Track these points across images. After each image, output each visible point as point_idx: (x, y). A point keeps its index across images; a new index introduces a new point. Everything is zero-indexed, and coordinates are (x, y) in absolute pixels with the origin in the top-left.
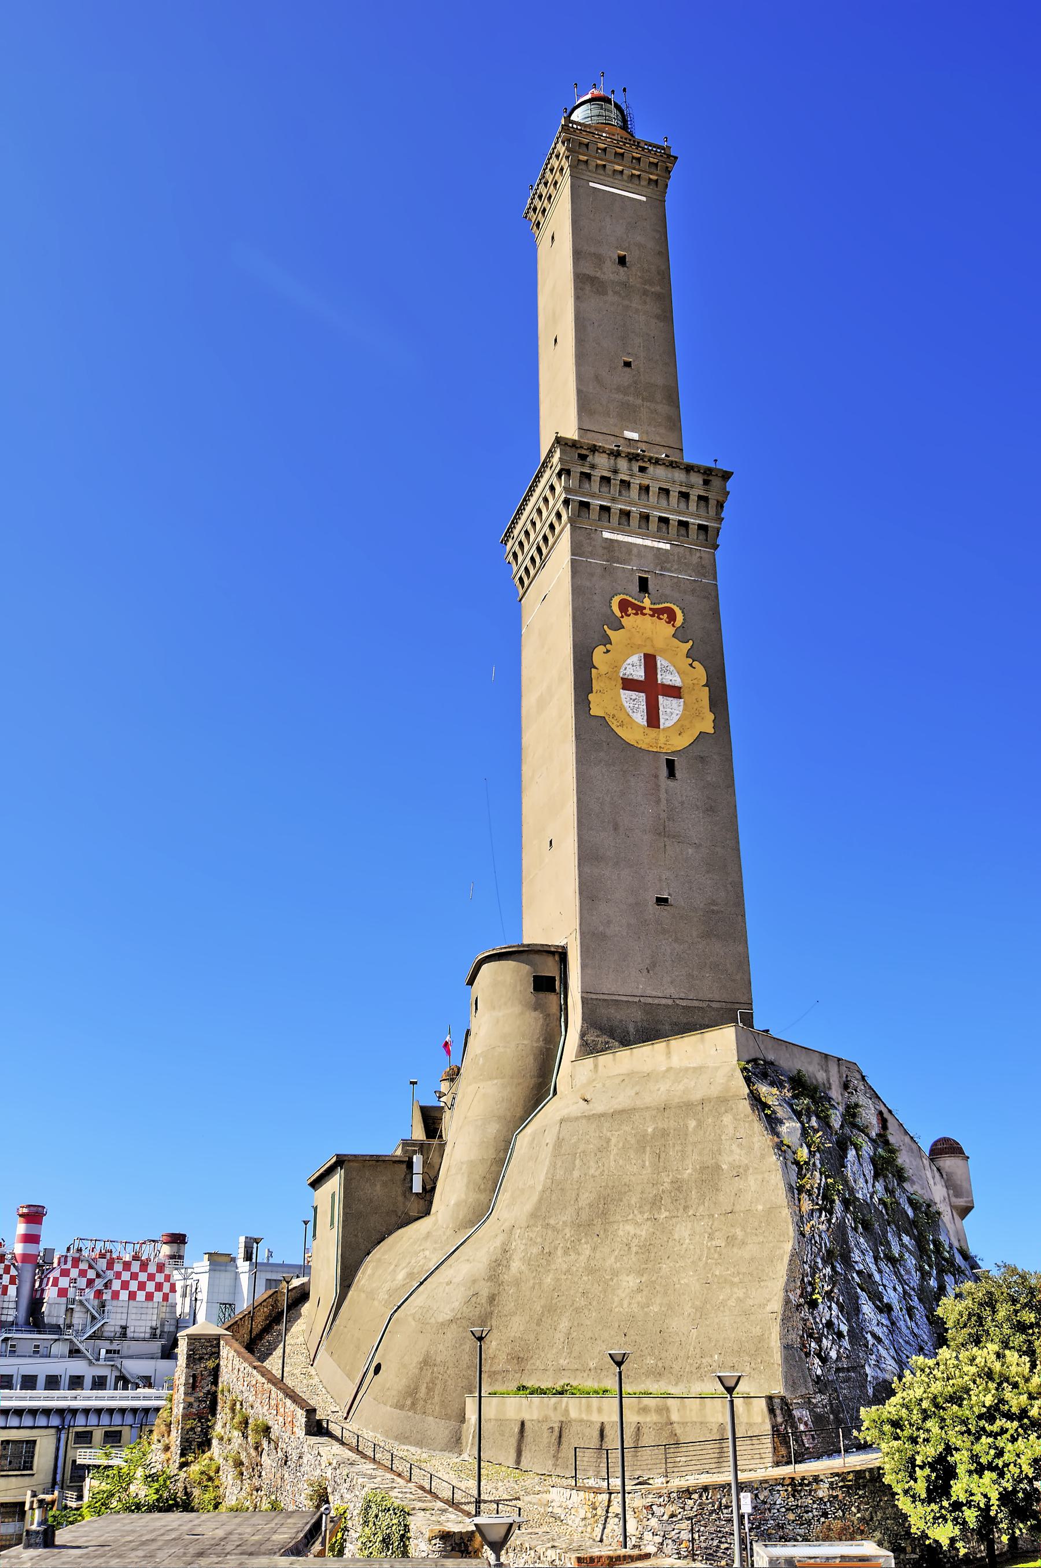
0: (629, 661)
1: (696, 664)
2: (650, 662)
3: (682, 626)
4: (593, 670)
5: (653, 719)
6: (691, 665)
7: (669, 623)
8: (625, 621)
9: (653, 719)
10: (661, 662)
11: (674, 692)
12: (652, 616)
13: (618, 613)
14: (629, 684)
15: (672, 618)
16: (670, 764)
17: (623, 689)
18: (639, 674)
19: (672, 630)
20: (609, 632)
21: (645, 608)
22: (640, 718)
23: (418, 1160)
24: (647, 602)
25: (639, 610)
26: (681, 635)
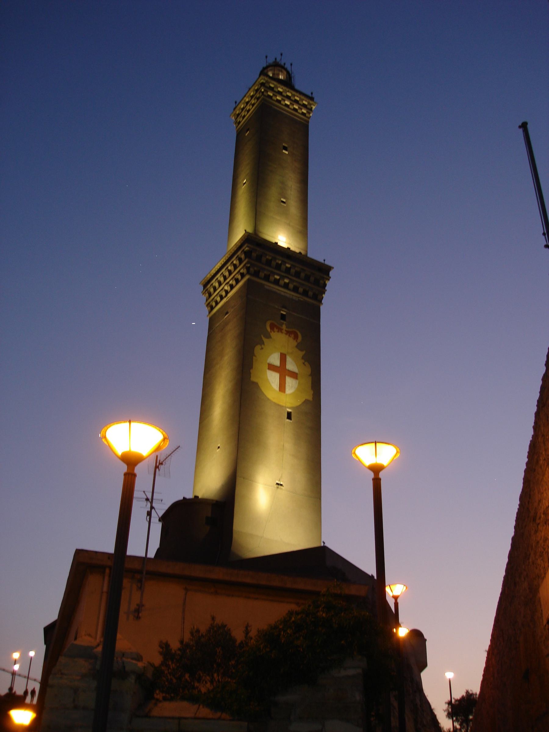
1: (306, 363)
2: (283, 358)
4: (254, 357)
5: (282, 388)
6: (304, 363)
8: (273, 334)
9: (282, 388)
10: (289, 359)
11: (294, 375)
12: (286, 334)
14: (272, 367)
17: (269, 369)
18: (277, 363)
19: (295, 344)
25: (280, 330)
26: (299, 347)
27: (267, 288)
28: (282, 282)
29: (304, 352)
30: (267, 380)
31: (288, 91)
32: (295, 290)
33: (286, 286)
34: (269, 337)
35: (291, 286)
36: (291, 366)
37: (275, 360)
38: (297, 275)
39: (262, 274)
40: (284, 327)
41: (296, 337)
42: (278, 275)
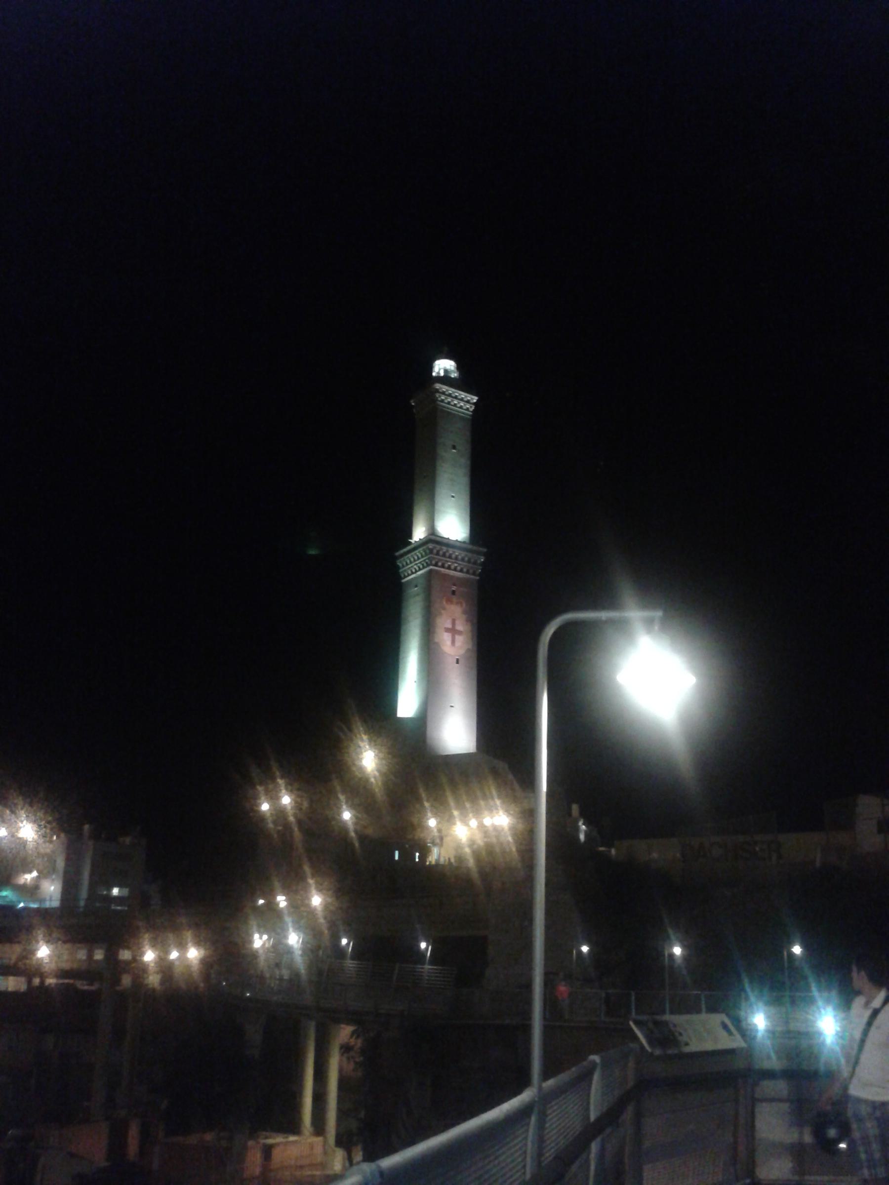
5: (453, 642)
10: (457, 622)
11: (460, 633)
14: (447, 630)
18: (449, 626)
26: (465, 612)
28: (453, 567)
32: (461, 571)
33: (455, 569)
34: (444, 609)
36: (460, 627)
37: (449, 625)
38: (463, 560)
39: (440, 564)
41: (462, 606)
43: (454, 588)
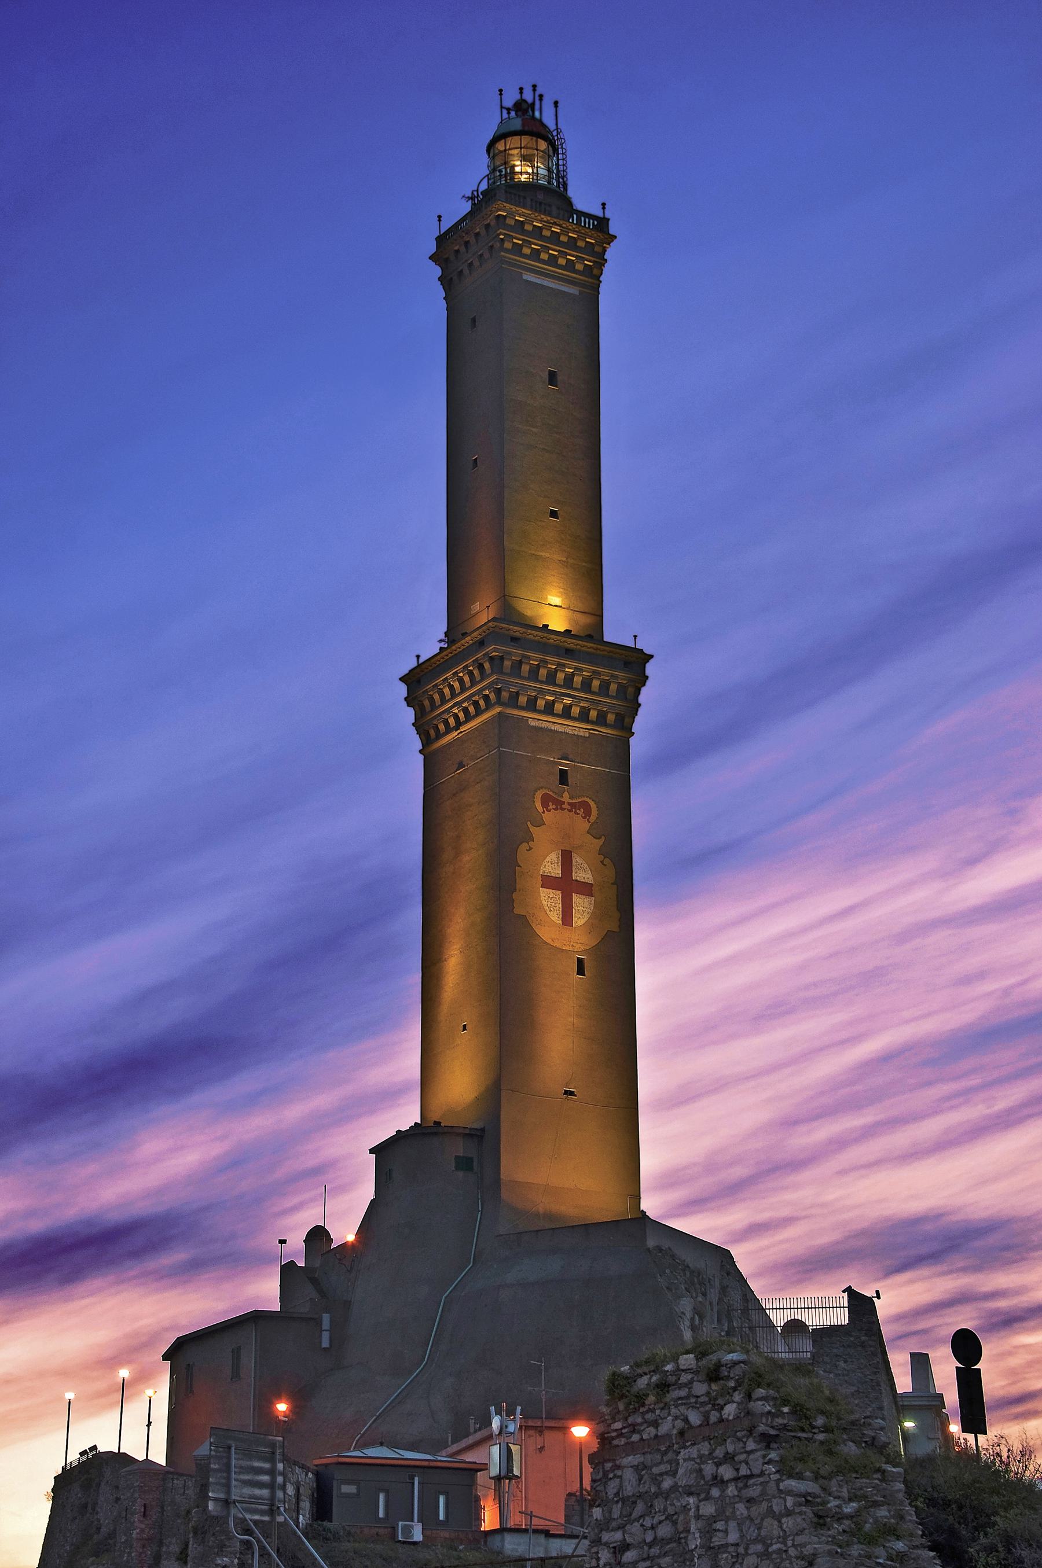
0: (548, 859)
1: (607, 861)
3: (596, 822)
6: (602, 862)
7: (584, 818)
10: (576, 859)
11: (586, 889)
12: (570, 811)
13: (540, 809)
14: (548, 882)
15: (588, 813)
16: (580, 962)
18: (556, 871)
19: (587, 826)
20: (532, 829)
21: (564, 803)
22: (556, 916)
23: (326, 1319)
24: (566, 797)
25: (559, 805)
27: (532, 723)
29: (601, 842)
30: (541, 907)
31: (555, 224)
32: (584, 717)
33: (566, 713)
35: (575, 711)
37: (552, 867)
39: (523, 700)
40: (566, 797)
41: (588, 813)
42: (552, 693)
43: (565, 764)
